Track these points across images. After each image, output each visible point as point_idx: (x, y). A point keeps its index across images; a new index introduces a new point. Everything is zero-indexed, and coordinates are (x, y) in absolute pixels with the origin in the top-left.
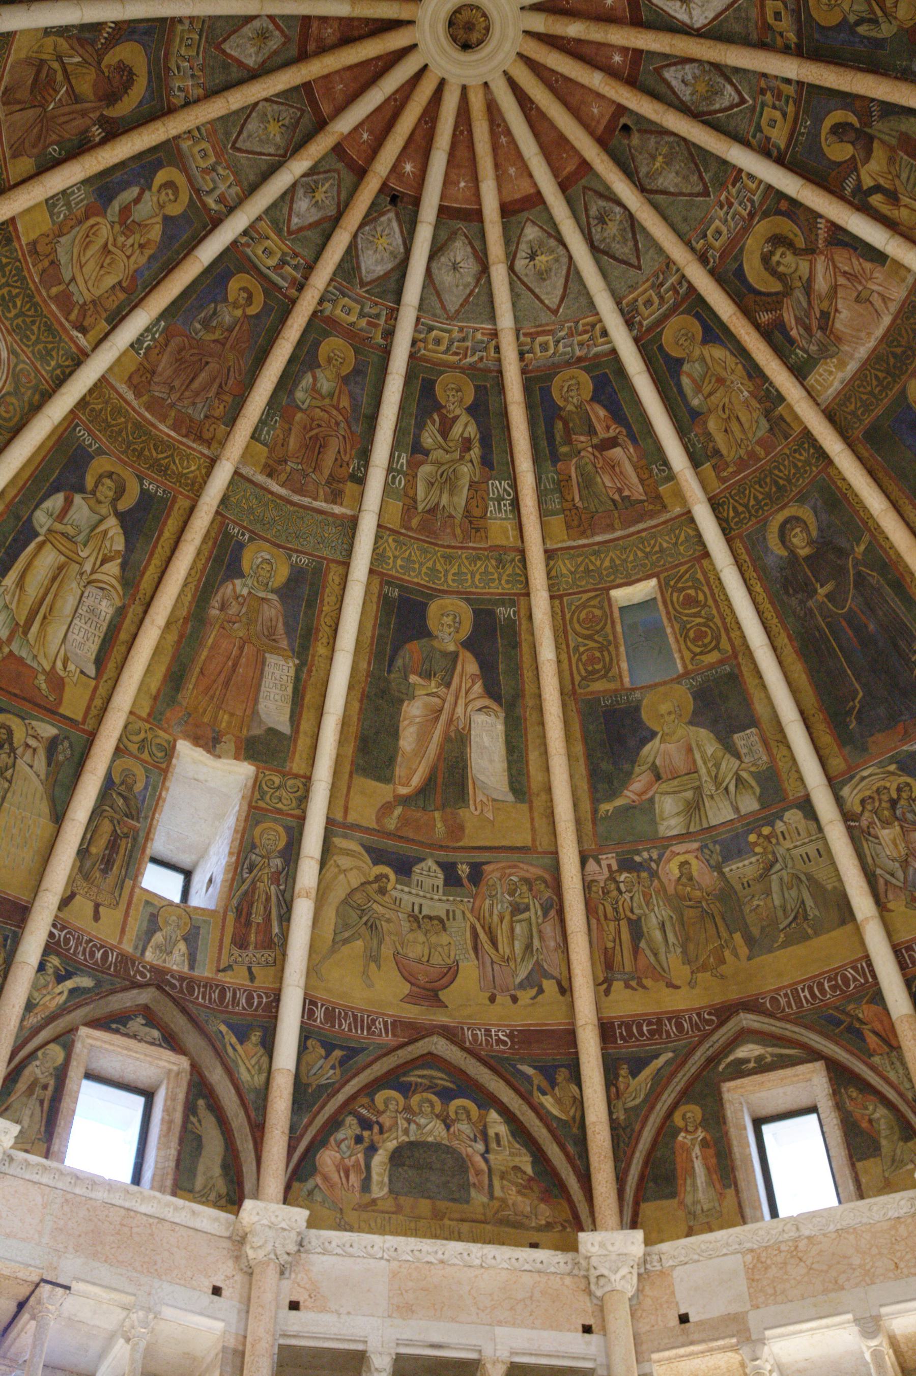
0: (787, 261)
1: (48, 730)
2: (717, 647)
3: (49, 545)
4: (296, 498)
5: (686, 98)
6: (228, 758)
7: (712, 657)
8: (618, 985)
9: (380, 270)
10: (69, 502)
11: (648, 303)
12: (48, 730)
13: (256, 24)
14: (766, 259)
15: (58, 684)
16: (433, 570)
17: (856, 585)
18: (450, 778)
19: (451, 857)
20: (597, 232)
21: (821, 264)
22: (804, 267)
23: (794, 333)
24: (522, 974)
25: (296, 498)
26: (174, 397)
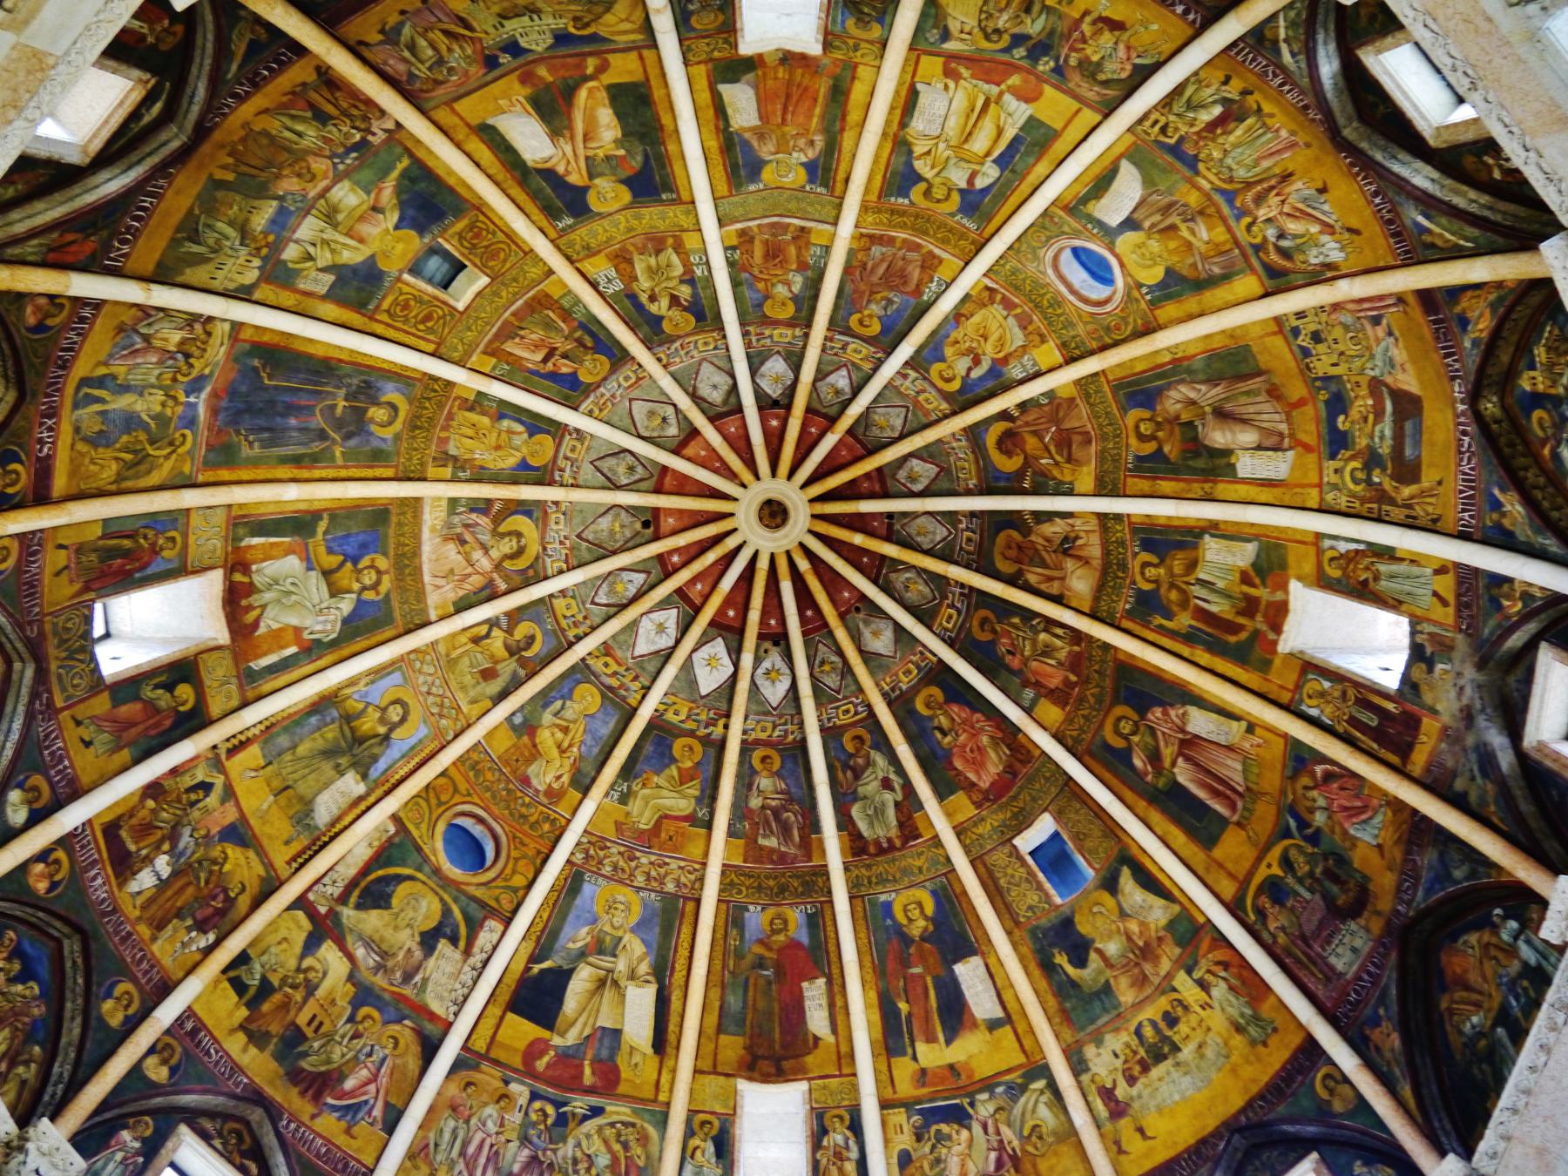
0: (508, 546)
1: (951, 46)
2: (388, 311)
3: (981, 154)
4: (775, 219)
5: (624, 574)
6: (770, 53)
7: (385, 305)
8: (311, 77)
9: (768, 364)
10: (971, 180)
11: (573, 450)
12: (951, 46)
13: (918, 487)
14: (519, 535)
15: (949, 73)
16: (639, 218)
17: (323, 431)
18: (552, 108)
19: (521, 60)
20: (630, 458)
21: (485, 564)
22: (495, 554)
23: (474, 516)
24: (407, 31)
25: (775, 219)
26: (901, 253)
